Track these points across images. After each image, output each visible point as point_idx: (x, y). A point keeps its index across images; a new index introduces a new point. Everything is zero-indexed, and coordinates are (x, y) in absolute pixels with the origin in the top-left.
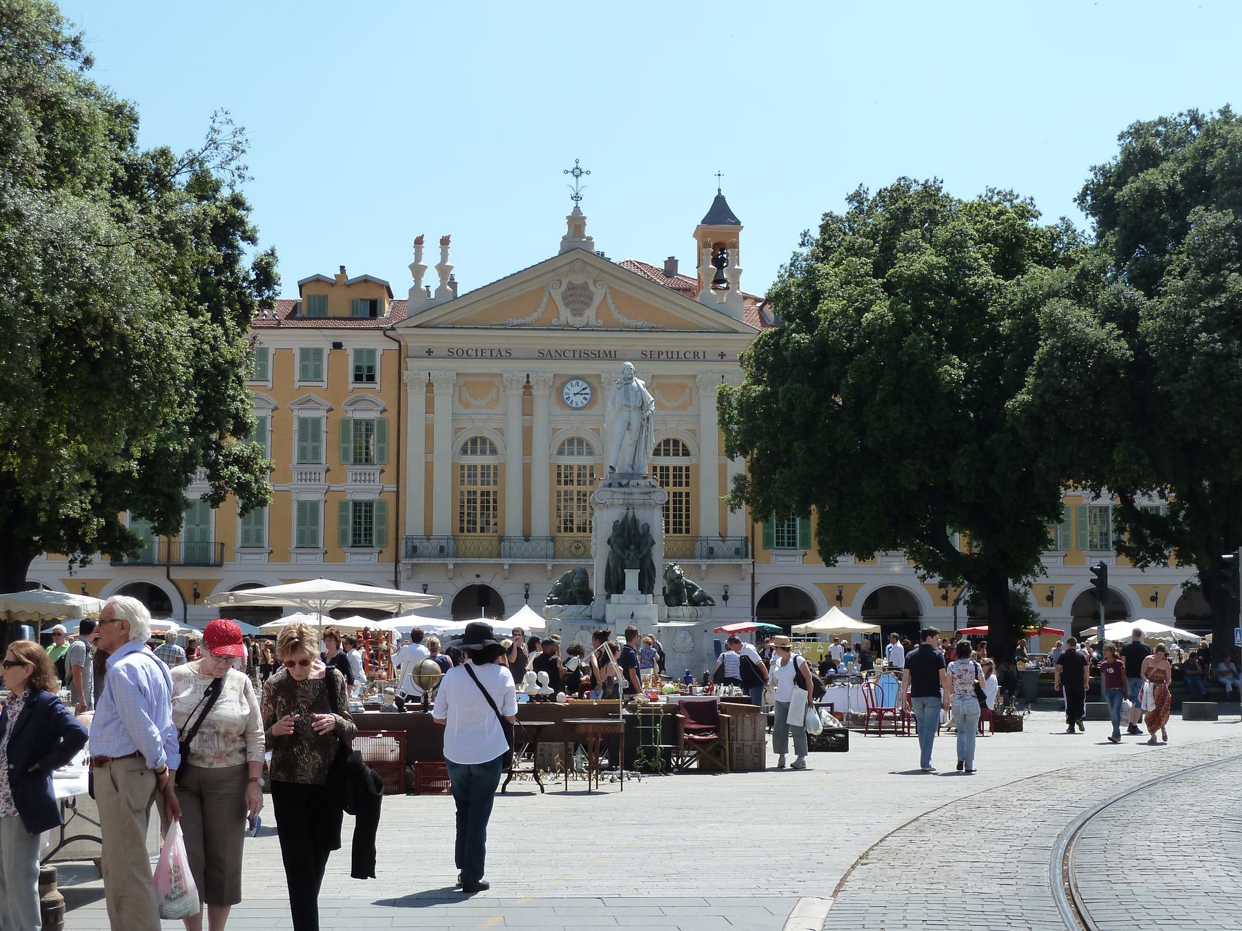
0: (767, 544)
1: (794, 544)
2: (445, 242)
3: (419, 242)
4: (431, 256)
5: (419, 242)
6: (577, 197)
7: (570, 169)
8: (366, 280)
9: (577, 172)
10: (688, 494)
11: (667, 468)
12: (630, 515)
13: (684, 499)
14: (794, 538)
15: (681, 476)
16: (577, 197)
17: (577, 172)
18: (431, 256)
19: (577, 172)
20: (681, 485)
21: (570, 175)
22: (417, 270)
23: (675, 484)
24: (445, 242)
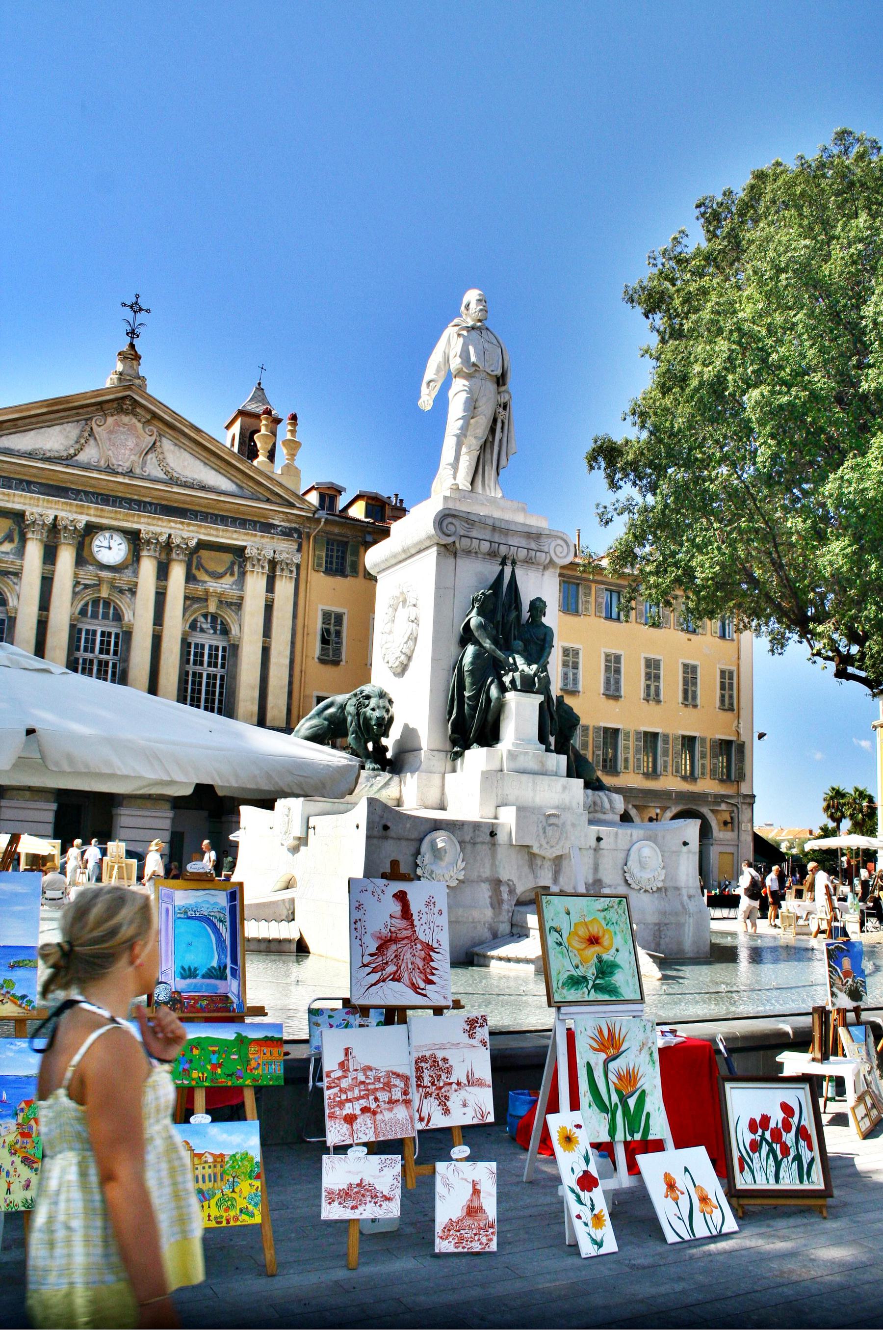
6: (132, 334)
7: (129, 303)
9: (136, 308)
11: (203, 646)
15: (217, 656)
16: (132, 334)
17: (136, 308)
19: (136, 308)
20: (216, 666)
21: (129, 309)
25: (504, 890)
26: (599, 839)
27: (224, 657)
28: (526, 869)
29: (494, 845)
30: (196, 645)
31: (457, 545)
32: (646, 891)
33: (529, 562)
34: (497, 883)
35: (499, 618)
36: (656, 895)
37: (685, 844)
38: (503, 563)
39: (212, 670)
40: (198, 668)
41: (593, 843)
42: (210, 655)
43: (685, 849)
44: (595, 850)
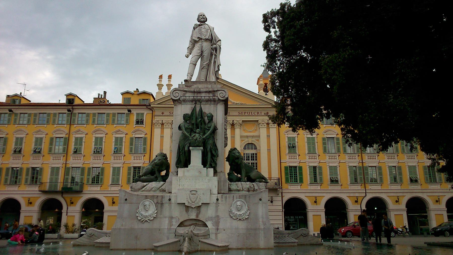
0: (287, 181)
1: (297, 181)
2: (170, 77)
3: (161, 77)
4: (165, 81)
5: (161, 77)
8: (144, 93)
10: (256, 163)
12: (198, 109)
13: (255, 165)
14: (297, 179)
15: (254, 157)
18: (165, 81)
20: (254, 160)
22: (160, 86)
23: (252, 160)
24: (170, 77)
25: (174, 220)
26: (217, 200)
27: (256, 157)
28: (185, 212)
29: (170, 203)
30: (247, 154)
31: (181, 99)
32: (240, 220)
33: (208, 101)
34: (172, 218)
35: (193, 122)
36: (245, 221)
37: (260, 200)
38: (196, 103)
39: (253, 161)
40: (253, 161)
41: (215, 201)
42: (251, 157)
43: (260, 202)
44: (216, 204)
